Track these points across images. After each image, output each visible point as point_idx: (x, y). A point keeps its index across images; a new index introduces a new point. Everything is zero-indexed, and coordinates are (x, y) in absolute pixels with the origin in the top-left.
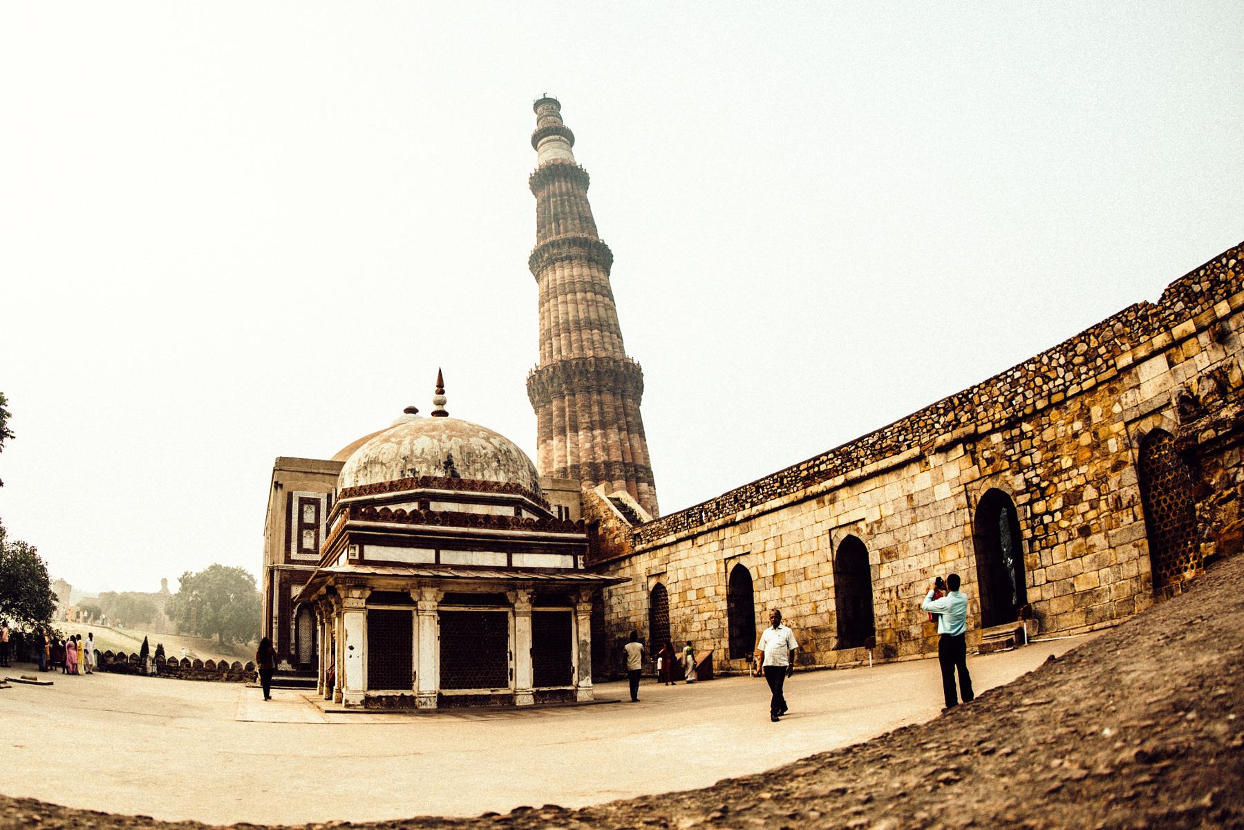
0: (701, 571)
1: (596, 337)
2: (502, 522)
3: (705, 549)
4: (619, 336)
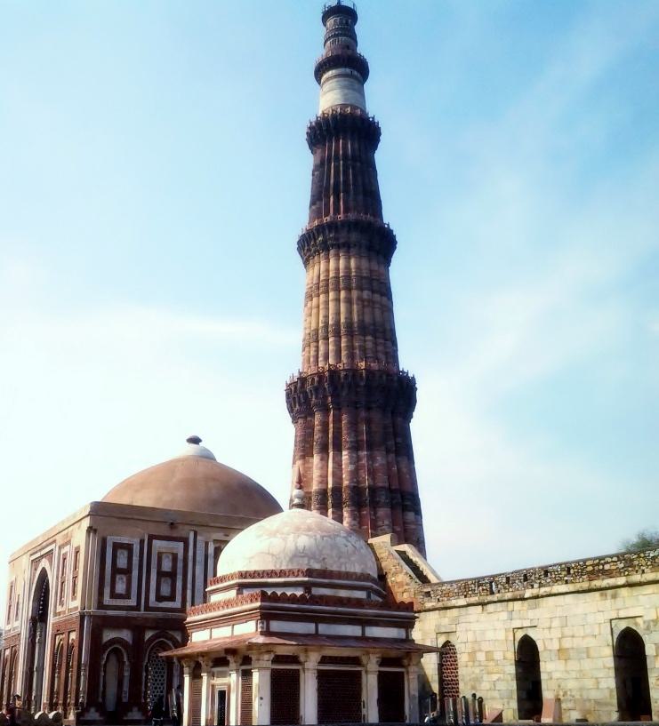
0: (490, 635)
1: (369, 345)
2: (359, 603)
3: (495, 616)
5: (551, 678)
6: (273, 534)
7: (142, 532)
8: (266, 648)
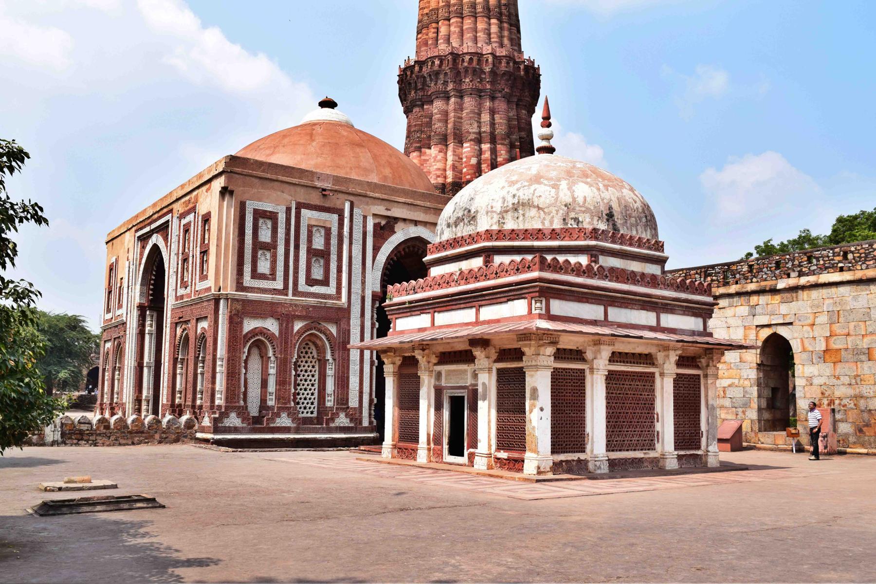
1: (494, 29)
3: (729, 312)
4: (519, 31)
5: (811, 384)
6: (537, 179)
7: (290, 198)
8: (550, 337)
